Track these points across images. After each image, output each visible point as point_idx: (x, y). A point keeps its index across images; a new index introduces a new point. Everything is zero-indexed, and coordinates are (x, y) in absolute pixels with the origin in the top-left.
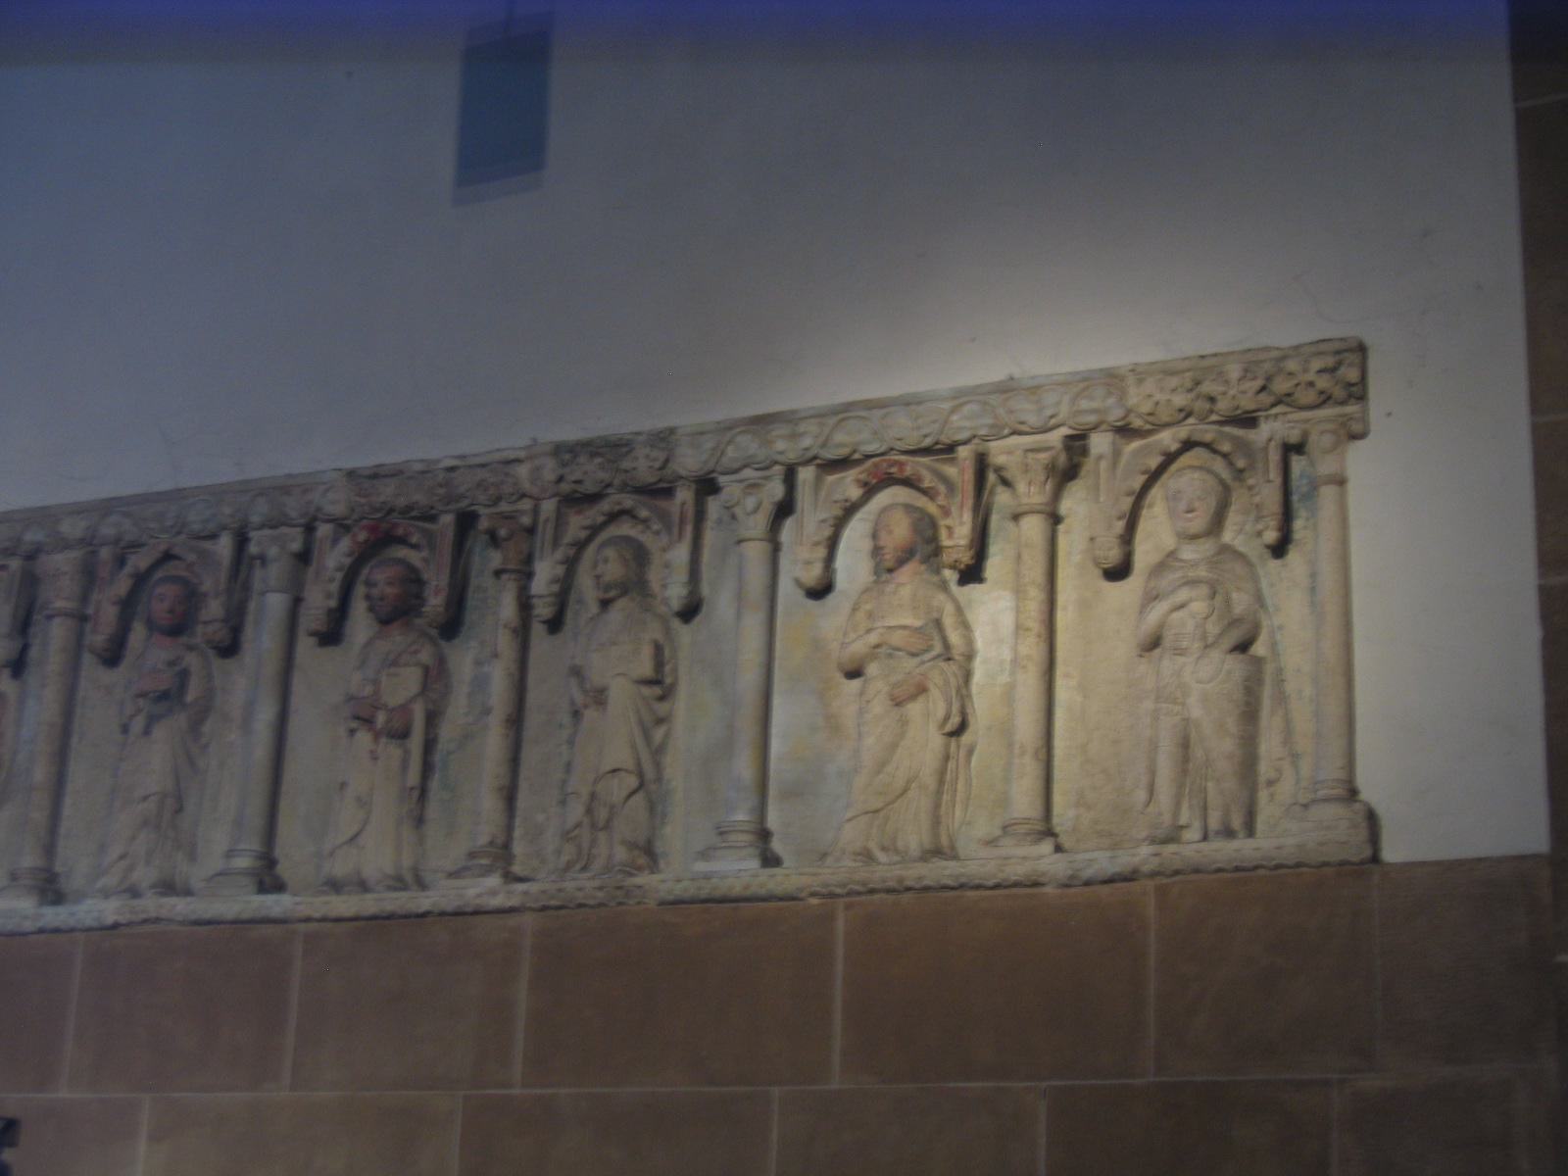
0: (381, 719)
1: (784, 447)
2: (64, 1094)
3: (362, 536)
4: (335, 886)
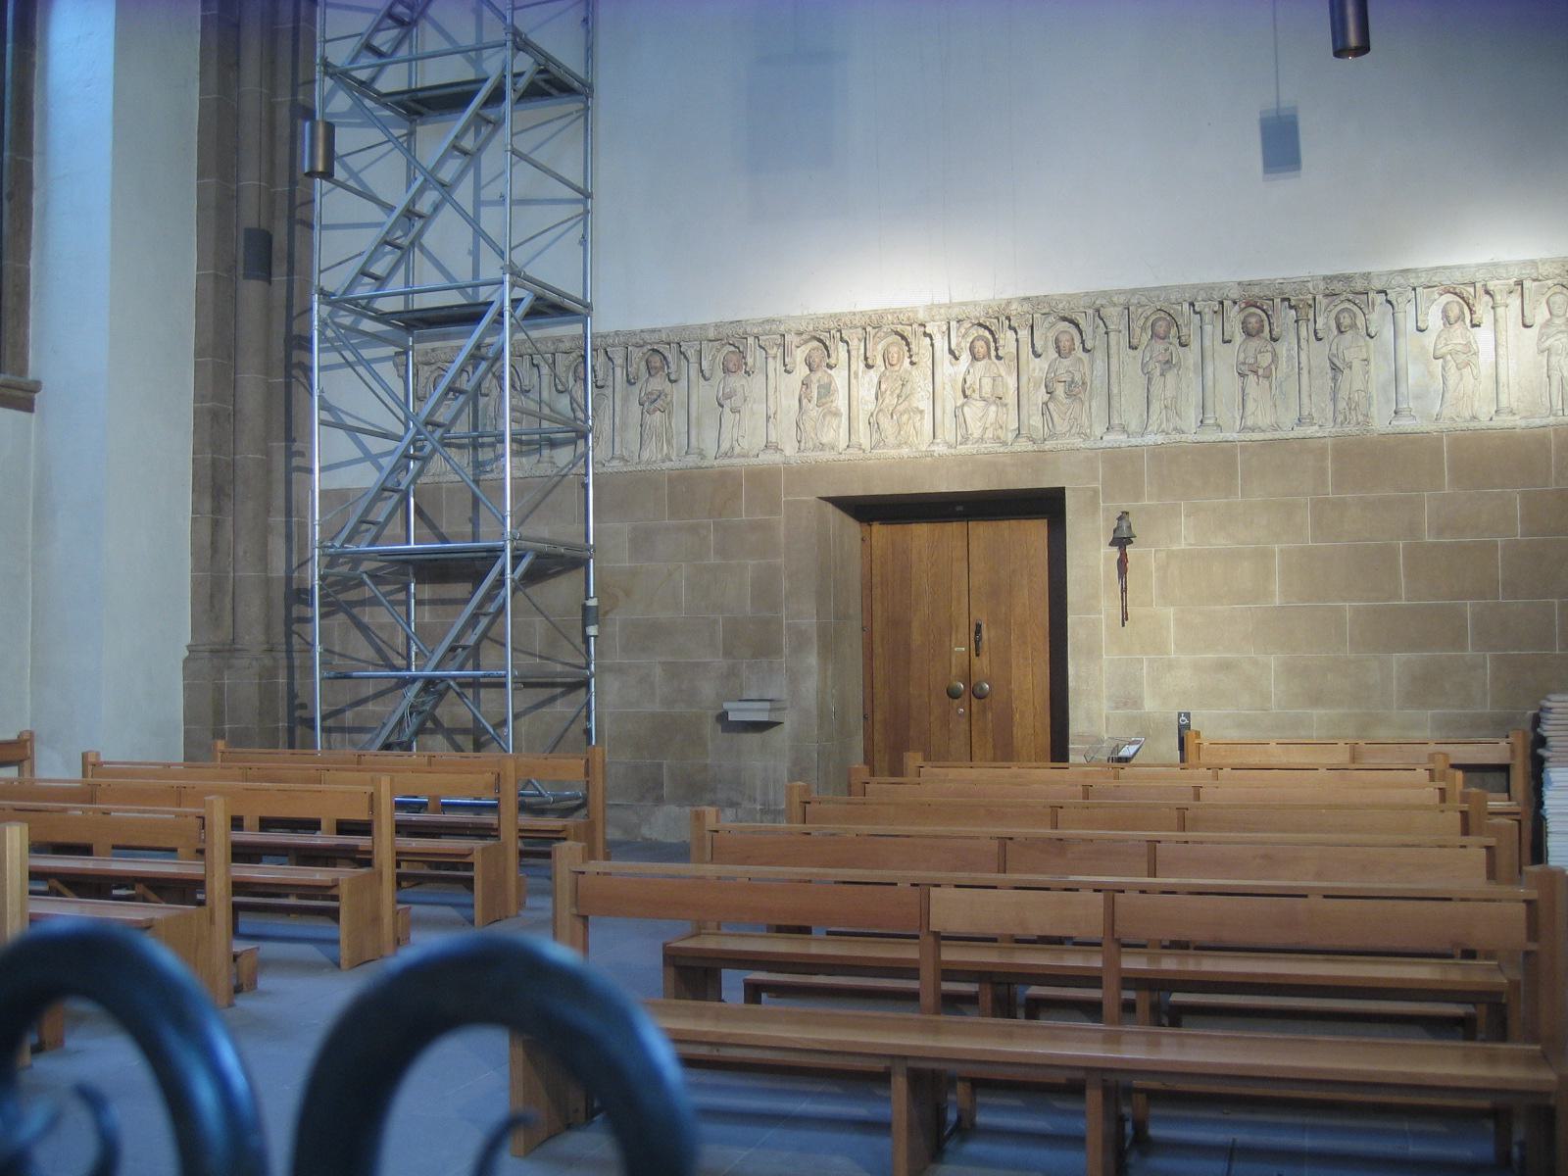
0: (1261, 372)
1: (1413, 281)
2: (1146, 502)
3: (1243, 306)
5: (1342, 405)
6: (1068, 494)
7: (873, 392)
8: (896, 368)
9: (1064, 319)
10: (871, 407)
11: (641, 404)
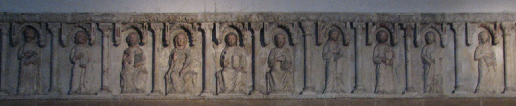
0: (388, 62)
3: (378, 26)
4: (383, 92)
5: (429, 82)
7: (167, 60)
8: (182, 48)
9: (281, 26)
10: (166, 69)
11: (20, 59)
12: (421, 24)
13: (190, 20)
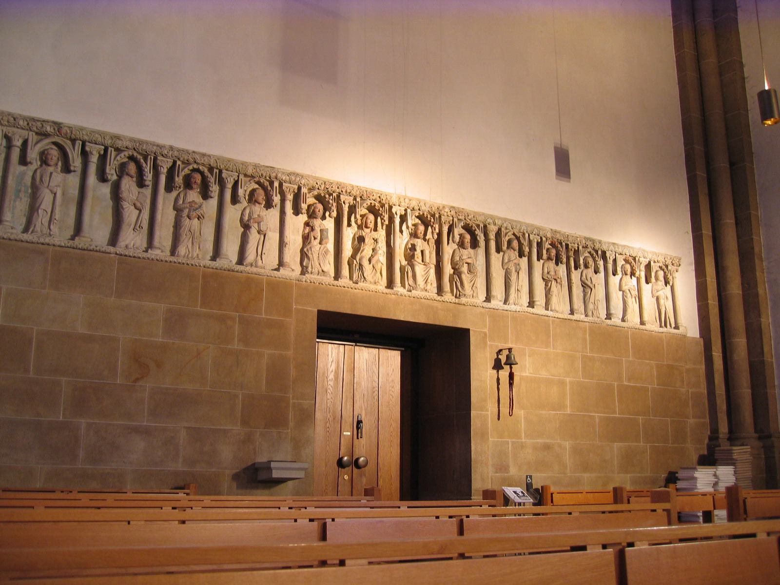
6: (471, 332)
12: (583, 247)
13: (384, 199)
